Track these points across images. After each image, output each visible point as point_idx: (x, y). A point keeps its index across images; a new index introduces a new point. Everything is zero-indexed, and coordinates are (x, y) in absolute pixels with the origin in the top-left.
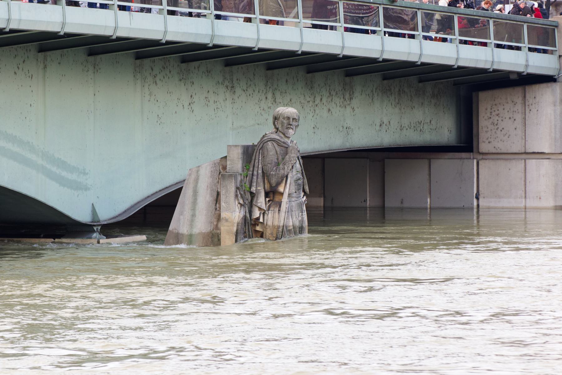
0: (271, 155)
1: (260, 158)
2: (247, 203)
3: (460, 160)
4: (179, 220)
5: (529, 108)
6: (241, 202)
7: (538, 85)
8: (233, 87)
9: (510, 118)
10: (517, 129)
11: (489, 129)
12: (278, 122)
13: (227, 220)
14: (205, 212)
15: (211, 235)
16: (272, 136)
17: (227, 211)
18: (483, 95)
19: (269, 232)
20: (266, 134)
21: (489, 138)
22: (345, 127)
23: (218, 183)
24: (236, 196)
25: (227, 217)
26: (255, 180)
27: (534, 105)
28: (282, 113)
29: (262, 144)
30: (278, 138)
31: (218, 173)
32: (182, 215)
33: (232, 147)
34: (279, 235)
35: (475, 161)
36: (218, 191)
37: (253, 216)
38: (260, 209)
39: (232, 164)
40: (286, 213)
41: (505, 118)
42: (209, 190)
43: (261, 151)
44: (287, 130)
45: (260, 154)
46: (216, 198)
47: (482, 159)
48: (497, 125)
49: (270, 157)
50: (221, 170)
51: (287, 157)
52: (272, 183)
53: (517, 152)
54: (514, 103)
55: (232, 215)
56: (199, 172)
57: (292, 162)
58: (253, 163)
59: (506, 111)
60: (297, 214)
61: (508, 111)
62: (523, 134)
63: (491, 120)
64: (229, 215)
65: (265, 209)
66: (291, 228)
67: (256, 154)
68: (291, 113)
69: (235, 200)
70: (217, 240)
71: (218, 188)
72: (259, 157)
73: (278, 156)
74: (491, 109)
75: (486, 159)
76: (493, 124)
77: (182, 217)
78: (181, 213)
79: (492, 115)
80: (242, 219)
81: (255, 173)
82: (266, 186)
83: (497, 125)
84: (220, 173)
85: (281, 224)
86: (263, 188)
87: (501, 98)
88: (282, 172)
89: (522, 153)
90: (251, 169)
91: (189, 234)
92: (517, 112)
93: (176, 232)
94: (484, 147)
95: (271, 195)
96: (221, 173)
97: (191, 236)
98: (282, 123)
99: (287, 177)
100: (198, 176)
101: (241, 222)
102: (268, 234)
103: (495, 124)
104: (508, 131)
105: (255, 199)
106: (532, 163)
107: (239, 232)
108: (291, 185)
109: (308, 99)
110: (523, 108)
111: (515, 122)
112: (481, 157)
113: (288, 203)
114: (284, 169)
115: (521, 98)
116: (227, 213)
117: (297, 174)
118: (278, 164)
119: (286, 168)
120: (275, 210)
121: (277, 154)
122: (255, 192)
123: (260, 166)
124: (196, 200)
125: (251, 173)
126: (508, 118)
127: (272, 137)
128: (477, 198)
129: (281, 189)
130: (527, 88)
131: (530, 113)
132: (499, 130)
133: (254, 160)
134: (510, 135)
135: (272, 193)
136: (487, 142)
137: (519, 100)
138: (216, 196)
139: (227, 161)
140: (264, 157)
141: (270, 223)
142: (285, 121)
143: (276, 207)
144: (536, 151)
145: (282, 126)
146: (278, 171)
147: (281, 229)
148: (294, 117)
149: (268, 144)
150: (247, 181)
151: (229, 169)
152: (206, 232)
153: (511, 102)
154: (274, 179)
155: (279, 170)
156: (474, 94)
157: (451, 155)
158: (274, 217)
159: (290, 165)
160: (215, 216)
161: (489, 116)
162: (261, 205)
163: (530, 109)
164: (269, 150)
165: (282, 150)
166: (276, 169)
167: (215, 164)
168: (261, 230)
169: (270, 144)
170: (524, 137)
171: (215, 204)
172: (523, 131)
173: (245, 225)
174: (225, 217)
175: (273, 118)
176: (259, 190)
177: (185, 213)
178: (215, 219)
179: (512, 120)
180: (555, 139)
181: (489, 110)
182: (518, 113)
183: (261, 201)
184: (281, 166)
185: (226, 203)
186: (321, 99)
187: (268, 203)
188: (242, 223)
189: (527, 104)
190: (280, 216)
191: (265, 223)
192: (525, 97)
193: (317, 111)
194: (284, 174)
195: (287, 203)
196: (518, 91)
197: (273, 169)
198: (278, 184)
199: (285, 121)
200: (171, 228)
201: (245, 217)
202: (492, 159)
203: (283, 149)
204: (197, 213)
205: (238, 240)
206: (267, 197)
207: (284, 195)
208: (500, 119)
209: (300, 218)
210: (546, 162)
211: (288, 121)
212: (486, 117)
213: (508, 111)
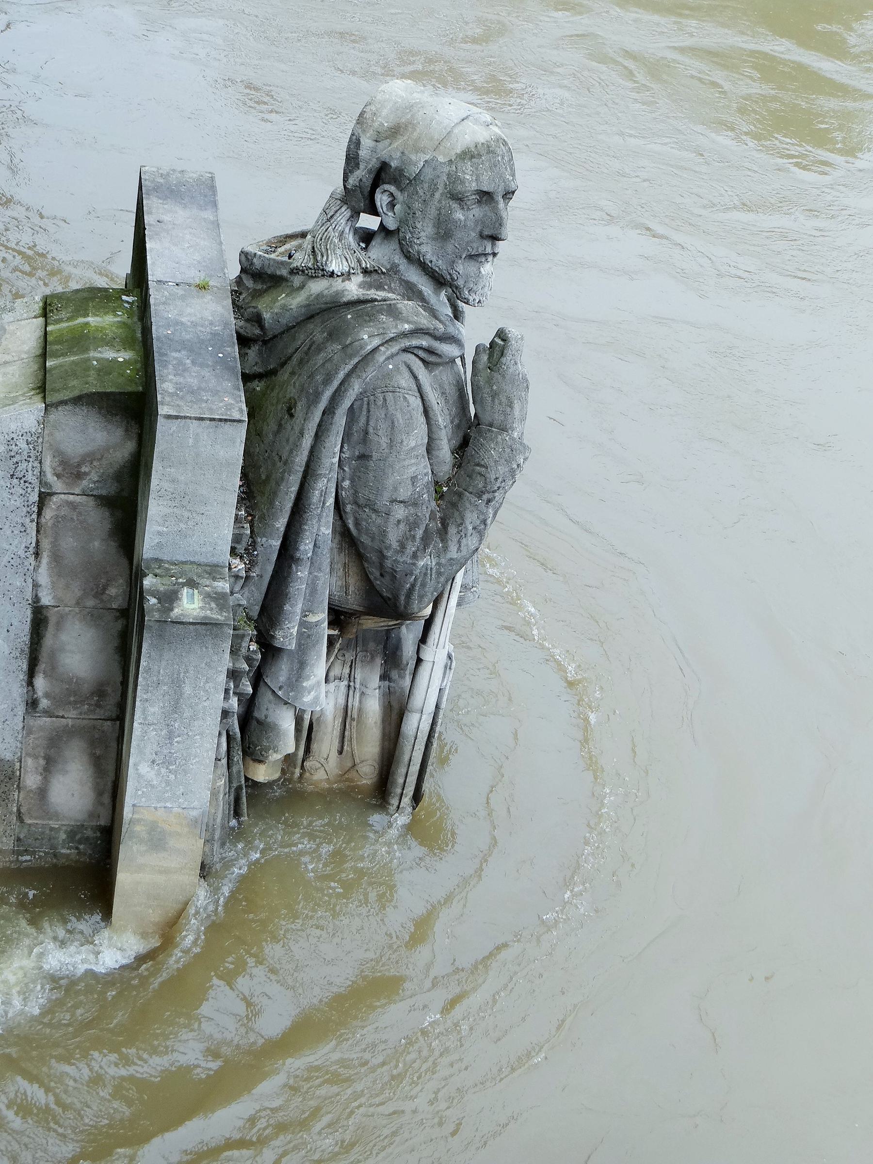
20: (320, 272)
23: (37, 554)
24: (225, 714)
31: (35, 497)
36: (36, 599)
37: (267, 749)
50: (50, 478)
58: (294, 489)
67: (319, 436)
71: (36, 586)
73: (430, 438)
81: (306, 547)
84: (43, 498)
90: (281, 523)
96: (55, 498)
119: (489, 521)
120: (358, 676)
125: (276, 543)
133: (300, 475)
138: (27, 628)
140: (363, 457)
151: (160, 545)
155: (459, 542)
162: (316, 699)
171: (22, 676)
175: (352, 160)
176: (317, 624)
185: (167, 762)
211: (476, 212)
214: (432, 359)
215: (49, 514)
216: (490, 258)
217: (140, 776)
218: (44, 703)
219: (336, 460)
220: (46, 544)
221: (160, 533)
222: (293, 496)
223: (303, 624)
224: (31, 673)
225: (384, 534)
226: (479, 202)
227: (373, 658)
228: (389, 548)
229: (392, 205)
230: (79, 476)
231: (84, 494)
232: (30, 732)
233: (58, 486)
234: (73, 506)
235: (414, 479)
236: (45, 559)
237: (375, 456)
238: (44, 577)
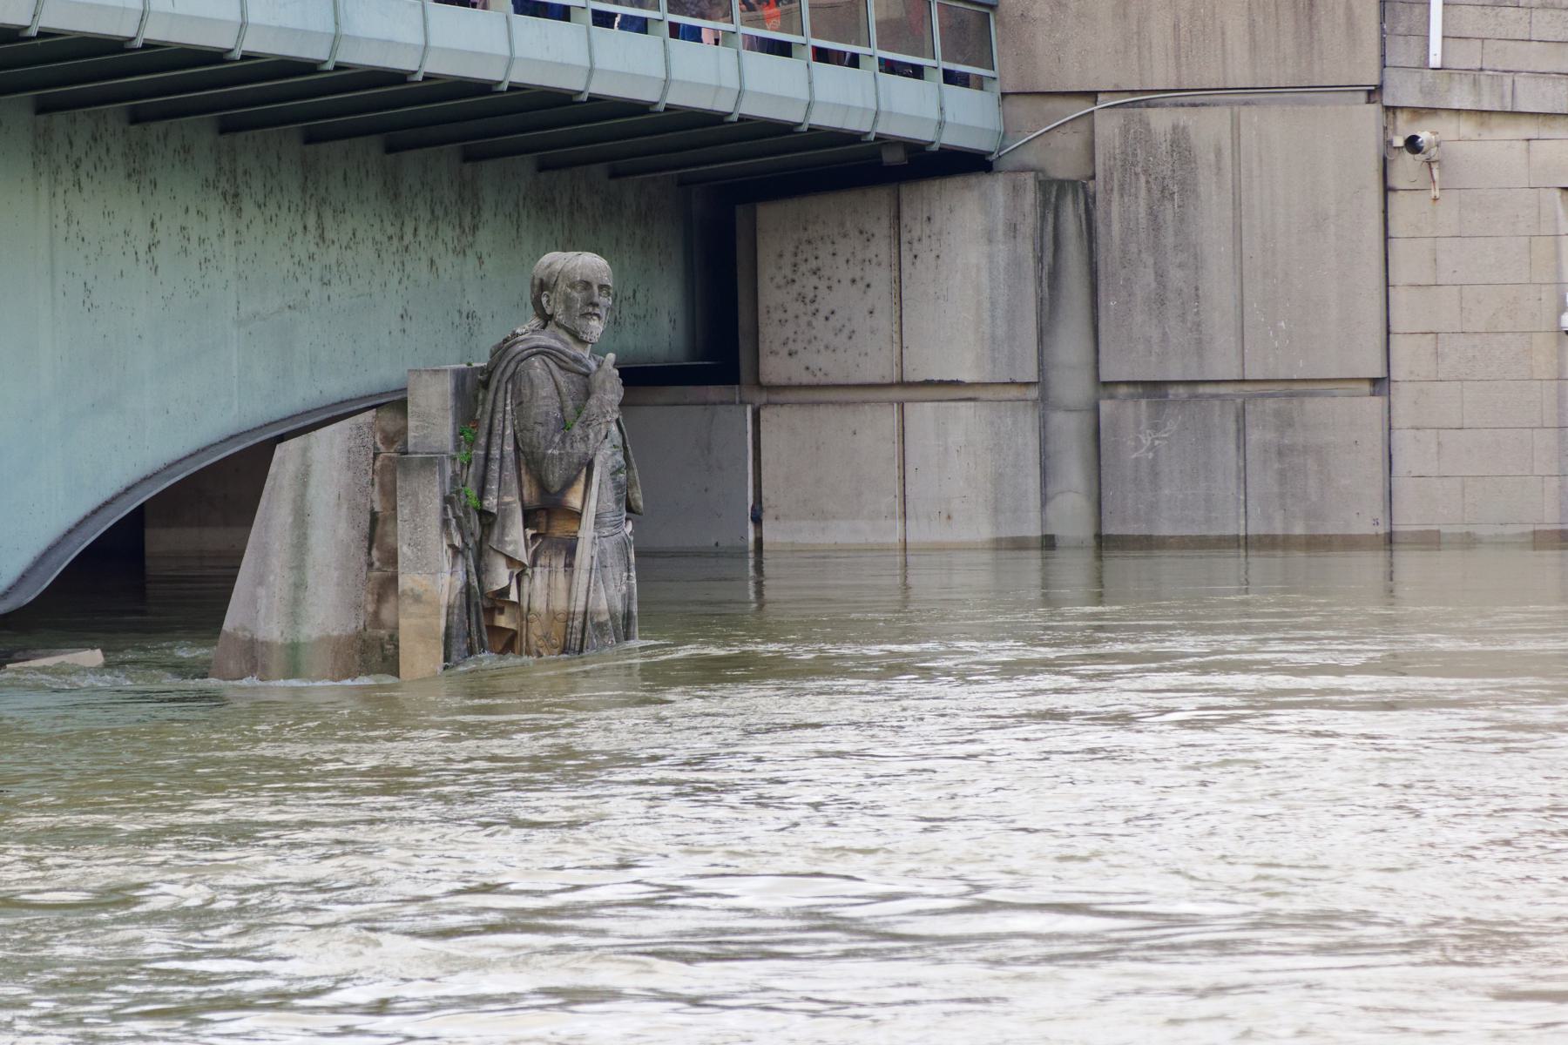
0: (544, 398)
1: (508, 408)
2: (470, 546)
3: (703, 407)
4: (253, 601)
5: (911, 250)
6: (457, 541)
7: (938, 182)
8: (236, 195)
9: (854, 281)
10: (876, 314)
11: (790, 315)
12: (552, 297)
13: (417, 599)
14: (335, 574)
15: (358, 644)
16: (540, 339)
17: (416, 569)
18: (768, 214)
19: (539, 632)
20: (515, 335)
21: (790, 342)
22: (464, 315)
23: (373, 485)
24: (445, 523)
25: (419, 589)
26: (497, 475)
27: (925, 241)
28: (566, 270)
29: (513, 365)
30: (558, 345)
31: (371, 455)
32: (261, 583)
33: (425, 377)
34: (573, 641)
35: (749, 409)
36: (372, 509)
37: (492, 584)
38: (511, 561)
39: (423, 428)
40: (593, 571)
41: (839, 281)
42: (345, 506)
43: (510, 386)
44: (584, 322)
45: (509, 396)
46: (368, 530)
47: (768, 403)
48: (813, 301)
49: (541, 403)
50: (379, 445)
51: (593, 401)
52: (552, 483)
53: (878, 380)
54: (865, 236)
55: (434, 582)
56: (309, 454)
57: (609, 419)
59: (841, 260)
60: (617, 577)
61: (848, 261)
62: (896, 328)
63: (796, 288)
64: (424, 582)
65: (526, 563)
66: (605, 617)
67: (496, 394)
68: (593, 270)
69: (442, 538)
70: (380, 659)
71: (372, 501)
72: (505, 405)
73: (562, 402)
74: (796, 255)
75: (782, 405)
76: (802, 298)
77: (261, 591)
78: (260, 580)
79: (799, 274)
80: (461, 593)
81: (495, 452)
82: (526, 492)
83: (813, 301)
85: (580, 608)
86: (517, 498)
87: (824, 223)
88: (580, 448)
89: (891, 385)
90: (482, 441)
91: (289, 641)
92: (874, 261)
93: (245, 636)
94: (775, 368)
95: (543, 520)
97: (294, 648)
98: (568, 302)
99: (590, 466)
100: (309, 466)
101: (458, 603)
102: (533, 639)
103: (807, 301)
104: (849, 320)
105: (496, 531)
106: (922, 414)
107: (454, 632)
108: (603, 486)
109: (390, 230)
110: (895, 251)
111: (871, 292)
112: (762, 397)
113: (597, 541)
114: (585, 438)
115: (885, 222)
116: (417, 577)
117: (614, 454)
118: (564, 426)
119: (592, 436)
120: (553, 564)
121: (559, 393)
122: (495, 511)
123: (508, 431)
124: (306, 539)
125: (482, 453)
126: (846, 282)
127: (540, 343)
128: (757, 520)
129: (574, 500)
130: (905, 190)
131: (913, 264)
132: (821, 316)
134: (853, 332)
135: (544, 513)
136: (784, 352)
137: (882, 229)
138: (368, 524)
139: (409, 419)
140: (521, 403)
141: (539, 604)
142: (575, 294)
143: (557, 554)
144: (937, 378)
145: (568, 308)
146: (568, 445)
147: (577, 623)
148: (605, 283)
149: (531, 366)
150: (470, 478)
151: (415, 445)
152: (344, 634)
153: (857, 233)
154: (557, 470)
156: (740, 211)
157: (673, 392)
158: (553, 586)
159: (603, 426)
160: (370, 585)
161: (790, 276)
162: (515, 551)
163: (915, 252)
164: (536, 381)
165: (573, 382)
166: (563, 441)
167: (359, 428)
168: (512, 626)
169: (537, 364)
170: (896, 337)
171: (366, 550)
172: (896, 318)
173: (468, 613)
174: (412, 590)
175: (533, 285)
176: (508, 503)
177: (272, 578)
178: (370, 597)
179: (861, 285)
180: (993, 338)
181: (788, 259)
182: (879, 264)
183: (516, 537)
184: (577, 431)
185: (416, 545)
186: (416, 230)
187: (533, 545)
188: (461, 605)
189: (904, 239)
190: (575, 581)
191: (525, 604)
192: (898, 217)
193: (408, 268)
194: (586, 454)
195: (593, 543)
196: (880, 197)
197: (552, 441)
198: (568, 484)
199: (577, 295)
200: (228, 625)
201: (468, 585)
202: (801, 404)
203: (575, 379)
205: (454, 657)
206: (531, 527)
207: (584, 519)
208: (822, 285)
209: (624, 588)
210: (965, 409)
212: (779, 280)
213: (848, 261)
214: (559, 362)
215: (378, 464)
216: (595, 318)
217: (404, 554)
218: (377, 564)
219: (508, 408)
220: (377, 479)
221: (415, 437)
222: (487, 426)
224: (370, 549)
225: (531, 440)
226: (585, 289)
227: (560, 553)
228: (534, 447)
229: (548, 302)
230: (393, 443)
231: (395, 452)
232: (369, 581)
233: (382, 448)
234: (390, 459)
235: (547, 414)
236: (377, 487)
237: (525, 400)
238: (376, 496)
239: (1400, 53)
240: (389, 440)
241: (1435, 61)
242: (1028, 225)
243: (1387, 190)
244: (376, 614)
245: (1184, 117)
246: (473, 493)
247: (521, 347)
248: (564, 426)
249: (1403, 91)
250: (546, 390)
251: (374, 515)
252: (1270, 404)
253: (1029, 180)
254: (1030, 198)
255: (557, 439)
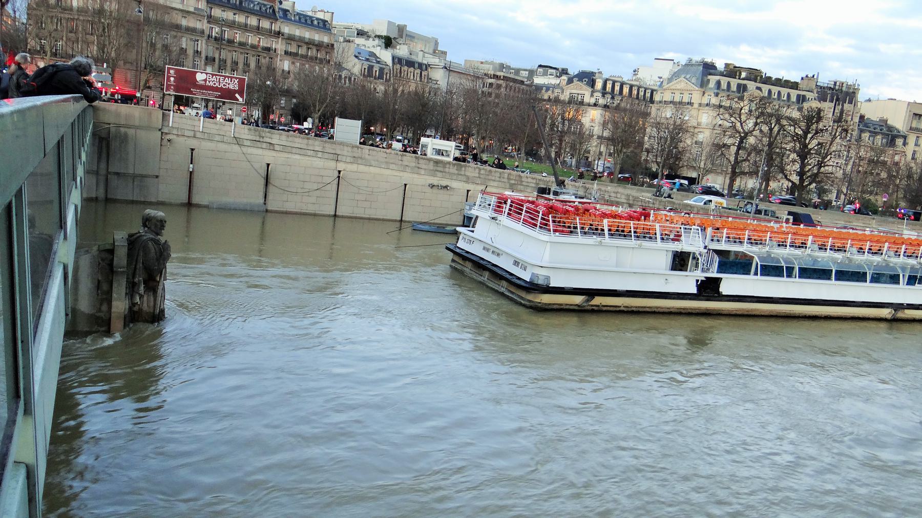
24: (126, 288)
81: (138, 267)
90: (134, 263)
105: (136, 288)
116: (117, 302)
140: (146, 254)
142: (158, 224)
166: (158, 264)
183: (142, 289)
184: (161, 262)
198: (157, 276)
204: (80, 298)
223: (139, 280)
239: (166, 124)
240: (103, 260)
241: (170, 125)
242: (97, 144)
243: (161, 145)
244: (100, 309)
245: (126, 130)
246: (131, 278)
247: (145, 238)
248: (158, 260)
249: (165, 130)
250: (153, 251)
251: (99, 281)
252: (139, 178)
253: (97, 137)
254: (97, 141)
255: (156, 264)
